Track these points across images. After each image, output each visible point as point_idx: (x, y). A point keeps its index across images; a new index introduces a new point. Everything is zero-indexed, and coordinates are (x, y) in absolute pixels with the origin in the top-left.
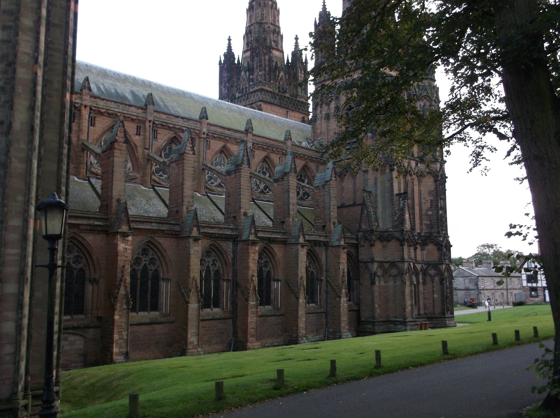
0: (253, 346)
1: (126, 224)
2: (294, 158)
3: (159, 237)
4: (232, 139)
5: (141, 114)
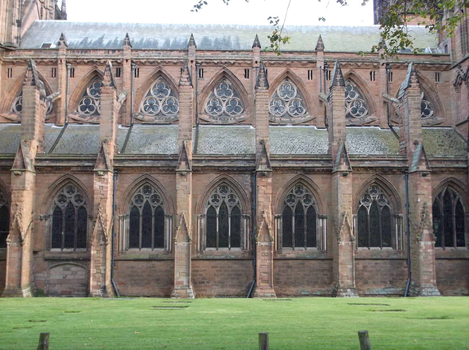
0: (264, 293)
1: (103, 163)
2: (340, 68)
3: (157, 173)
4: (295, 62)
5: (182, 56)
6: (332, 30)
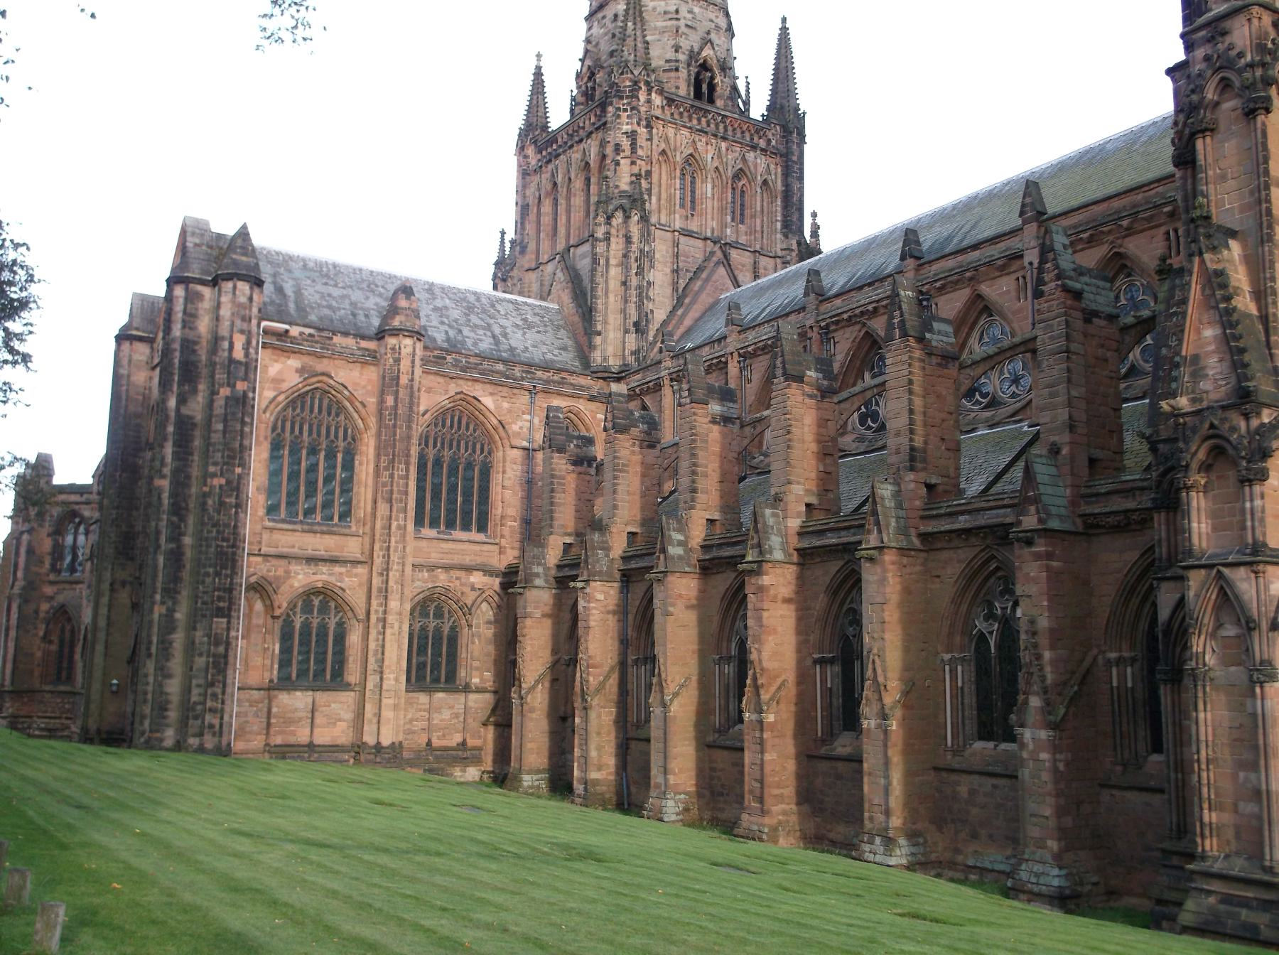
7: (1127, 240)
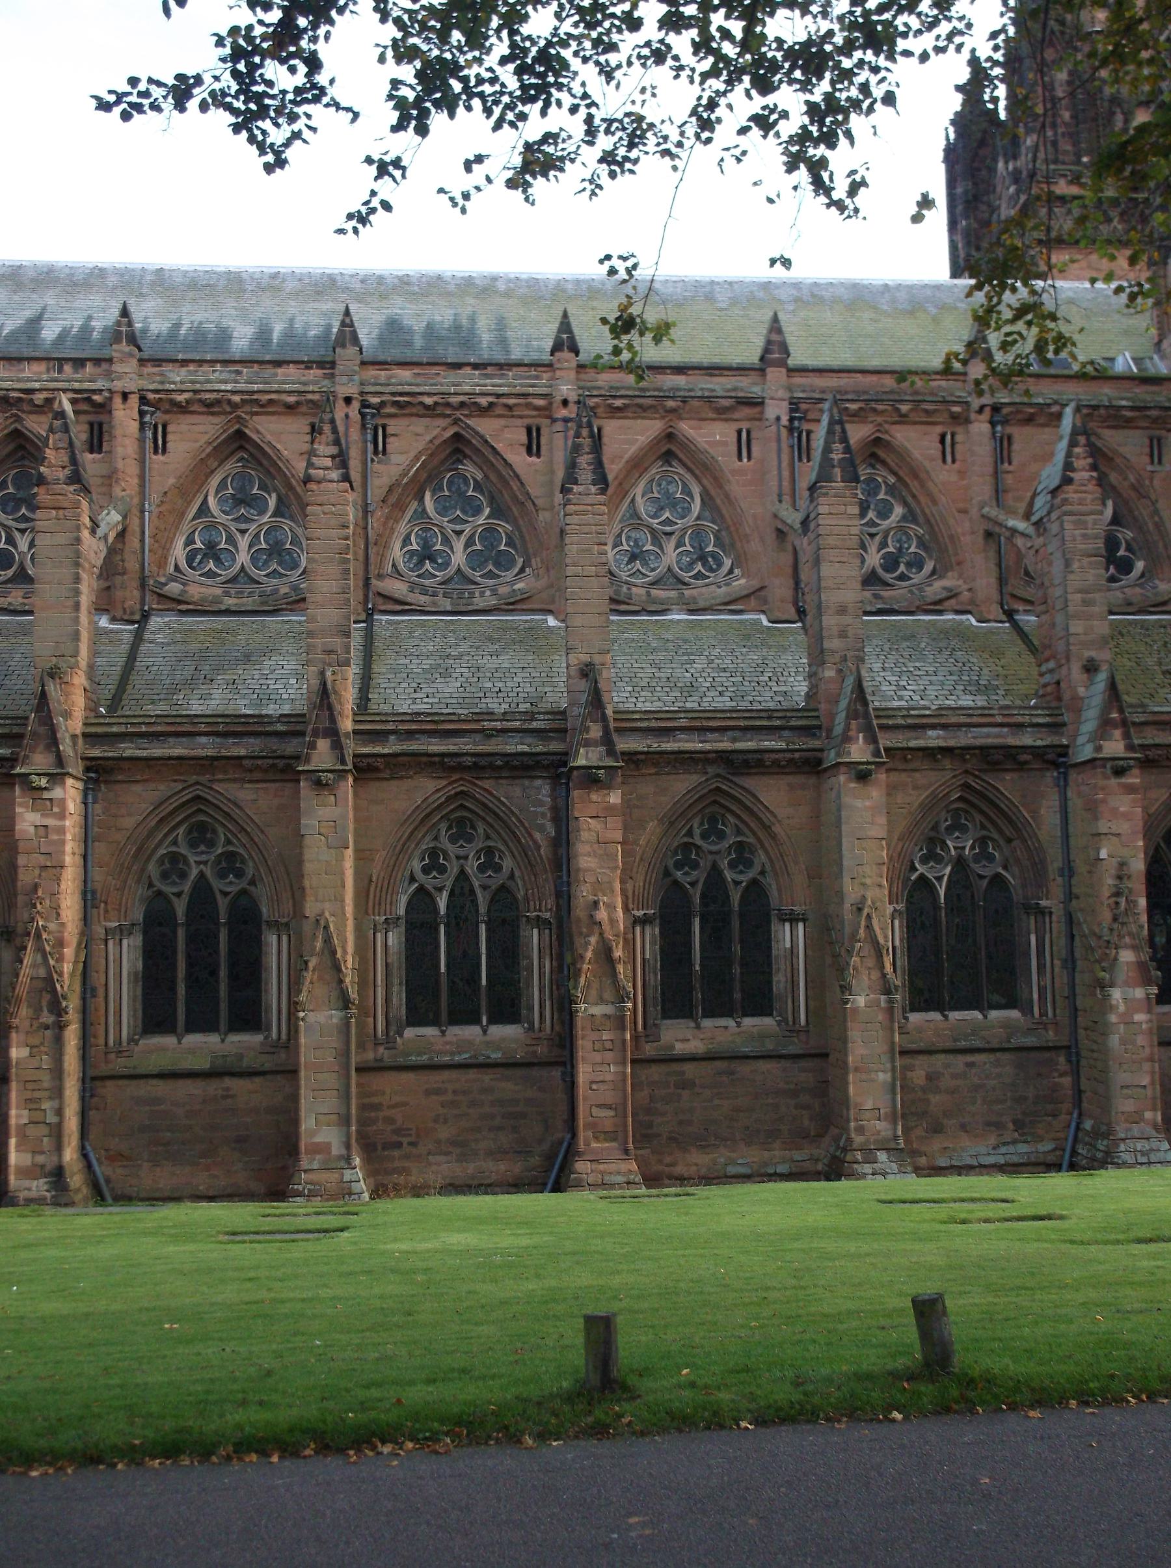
0: (602, 1173)
3: (235, 780)
4: (695, 403)
5: (315, 383)
6: (813, 295)
7: (897, 427)
